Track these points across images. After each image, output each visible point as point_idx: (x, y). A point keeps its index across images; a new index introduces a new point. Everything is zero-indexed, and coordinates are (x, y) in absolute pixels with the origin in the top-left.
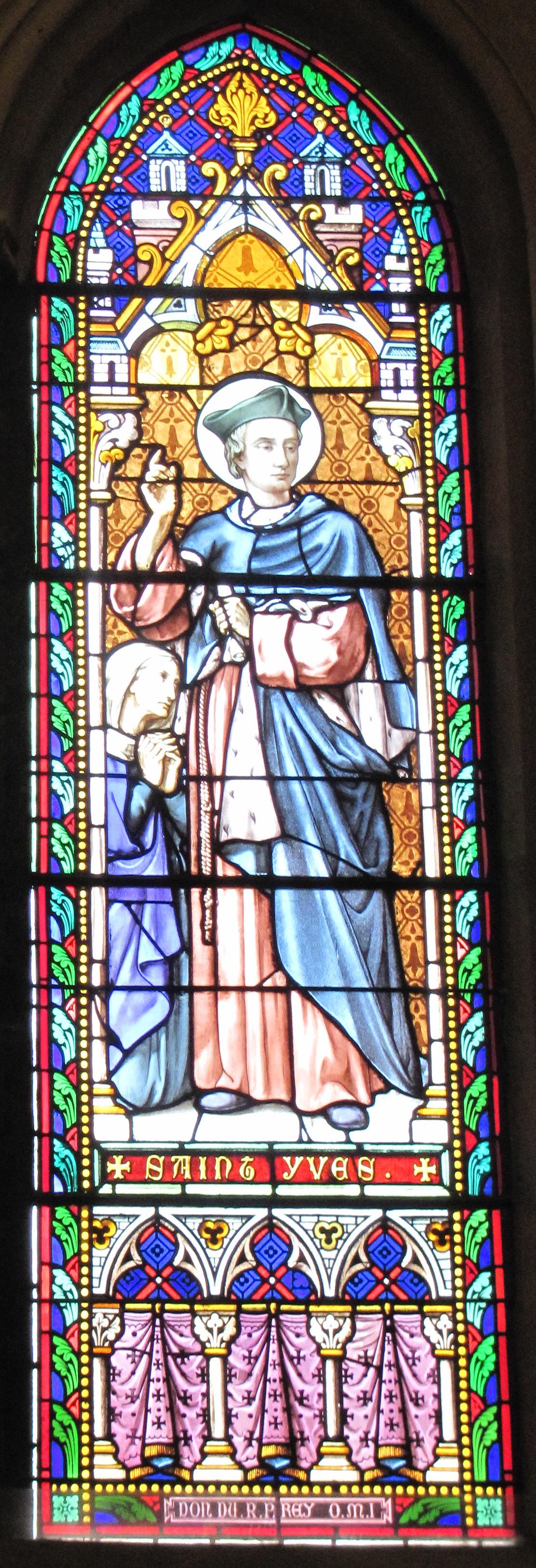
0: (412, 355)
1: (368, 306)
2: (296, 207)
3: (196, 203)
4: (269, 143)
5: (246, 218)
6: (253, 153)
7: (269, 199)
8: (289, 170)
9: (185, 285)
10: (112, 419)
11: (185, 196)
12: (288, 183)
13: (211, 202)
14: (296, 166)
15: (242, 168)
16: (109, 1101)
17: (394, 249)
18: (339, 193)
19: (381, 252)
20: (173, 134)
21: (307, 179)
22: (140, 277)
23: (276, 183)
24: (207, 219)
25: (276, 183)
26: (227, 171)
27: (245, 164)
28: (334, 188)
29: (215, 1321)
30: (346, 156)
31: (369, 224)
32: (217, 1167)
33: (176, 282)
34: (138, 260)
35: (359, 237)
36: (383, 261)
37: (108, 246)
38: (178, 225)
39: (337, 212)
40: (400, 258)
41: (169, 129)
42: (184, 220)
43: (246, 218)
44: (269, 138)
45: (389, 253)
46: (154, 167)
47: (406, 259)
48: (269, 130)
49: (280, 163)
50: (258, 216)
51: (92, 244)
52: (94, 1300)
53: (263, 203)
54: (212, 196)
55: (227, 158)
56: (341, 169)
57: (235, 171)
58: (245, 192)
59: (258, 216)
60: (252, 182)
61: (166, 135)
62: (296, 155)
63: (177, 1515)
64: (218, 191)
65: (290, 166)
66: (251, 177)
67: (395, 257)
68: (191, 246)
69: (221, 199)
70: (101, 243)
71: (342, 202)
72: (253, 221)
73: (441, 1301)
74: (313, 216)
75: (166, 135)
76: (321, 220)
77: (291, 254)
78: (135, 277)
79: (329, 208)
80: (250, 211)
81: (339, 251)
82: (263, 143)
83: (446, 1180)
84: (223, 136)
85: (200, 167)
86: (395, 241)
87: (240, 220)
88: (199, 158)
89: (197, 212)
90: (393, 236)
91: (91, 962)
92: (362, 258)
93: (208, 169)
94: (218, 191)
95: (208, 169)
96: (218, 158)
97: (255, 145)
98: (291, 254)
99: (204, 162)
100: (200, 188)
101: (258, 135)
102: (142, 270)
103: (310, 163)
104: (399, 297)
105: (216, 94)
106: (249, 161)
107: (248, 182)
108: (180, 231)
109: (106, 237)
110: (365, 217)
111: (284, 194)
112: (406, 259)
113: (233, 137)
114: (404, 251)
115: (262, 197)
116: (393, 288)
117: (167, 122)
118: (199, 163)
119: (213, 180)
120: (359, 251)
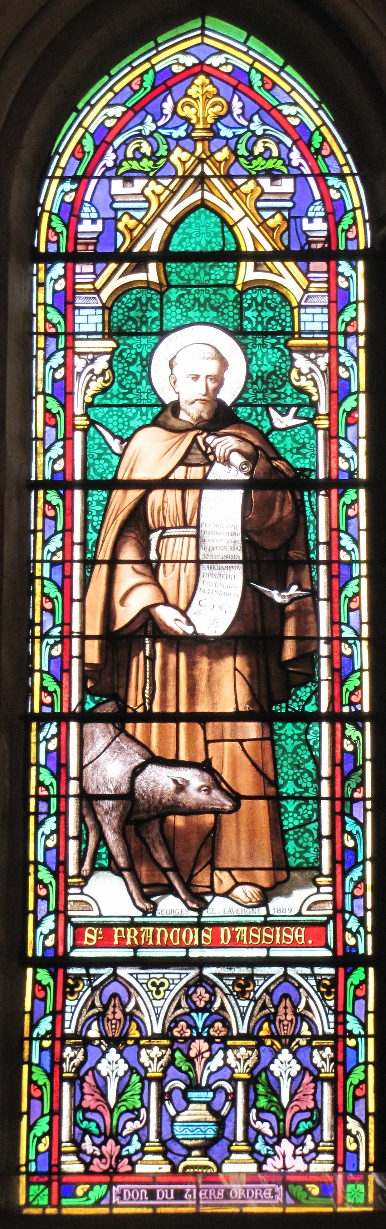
5: (203, 195)
7: (219, 177)
9: (151, 251)
22: (118, 246)
29: (156, 1052)
32: (158, 937)
33: (145, 249)
43: (203, 195)
52: (65, 1037)
53: (215, 181)
58: (202, 173)
63: (122, 1199)
72: (208, 196)
73: (326, 1037)
77: (236, 224)
80: (206, 187)
83: (331, 943)
87: (196, 197)
98: (236, 224)
115: (215, 176)
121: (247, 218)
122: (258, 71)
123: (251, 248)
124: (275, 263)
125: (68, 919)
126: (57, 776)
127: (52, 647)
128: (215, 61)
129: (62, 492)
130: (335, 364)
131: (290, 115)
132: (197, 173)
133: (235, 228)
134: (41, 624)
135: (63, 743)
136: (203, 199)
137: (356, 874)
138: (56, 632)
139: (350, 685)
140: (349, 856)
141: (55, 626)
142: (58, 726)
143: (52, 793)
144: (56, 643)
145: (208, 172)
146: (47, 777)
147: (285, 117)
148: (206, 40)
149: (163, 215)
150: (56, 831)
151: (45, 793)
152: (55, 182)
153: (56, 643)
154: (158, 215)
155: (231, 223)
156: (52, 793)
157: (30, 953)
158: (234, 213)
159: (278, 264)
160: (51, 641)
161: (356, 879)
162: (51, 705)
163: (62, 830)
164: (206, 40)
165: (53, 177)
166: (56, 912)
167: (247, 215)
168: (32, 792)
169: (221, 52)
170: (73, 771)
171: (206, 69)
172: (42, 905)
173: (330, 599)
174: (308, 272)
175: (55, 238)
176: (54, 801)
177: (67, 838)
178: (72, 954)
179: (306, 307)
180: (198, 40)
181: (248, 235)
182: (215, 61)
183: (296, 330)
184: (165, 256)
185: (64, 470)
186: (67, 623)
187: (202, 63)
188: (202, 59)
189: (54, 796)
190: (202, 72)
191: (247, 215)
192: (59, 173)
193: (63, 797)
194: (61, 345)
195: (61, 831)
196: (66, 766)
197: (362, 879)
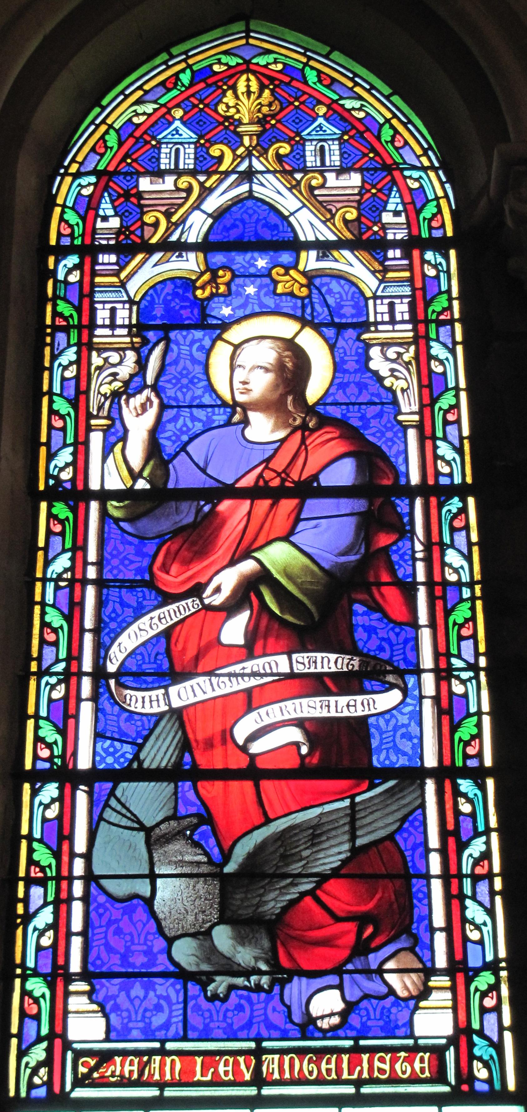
0: (407, 291)
1: (366, 255)
2: (298, 176)
3: (202, 178)
4: (273, 126)
5: (251, 187)
6: (259, 136)
8: (292, 146)
9: (189, 241)
10: (114, 357)
11: (193, 173)
12: (291, 157)
13: (215, 177)
14: (297, 142)
15: (247, 149)
16: (85, 999)
17: (391, 207)
18: (338, 163)
19: (378, 209)
20: (184, 123)
21: (308, 153)
23: (279, 158)
24: (211, 190)
25: (279, 158)
26: (234, 151)
27: (250, 146)
28: (334, 158)
30: (344, 133)
31: (368, 187)
34: (144, 224)
35: (358, 198)
36: (380, 216)
37: (116, 215)
38: (184, 195)
39: (337, 179)
40: (396, 213)
41: (181, 119)
42: (189, 190)
43: (251, 187)
44: (273, 122)
45: (385, 210)
46: (164, 150)
47: (403, 214)
48: (273, 117)
49: (284, 141)
50: (262, 185)
51: (101, 213)
54: (216, 172)
55: (234, 139)
56: (340, 144)
57: (240, 151)
58: (250, 166)
59: (262, 185)
60: (258, 158)
61: (177, 124)
62: (298, 134)
64: (223, 168)
65: (293, 142)
66: (257, 154)
67: (391, 214)
68: (197, 213)
69: (227, 174)
70: (110, 212)
71: (341, 171)
74: (314, 183)
75: (177, 124)
76: (323, 186)
77: (292, 214)
78: (142, 237)
79: (331, 177)
80: (255, 180)
81: (337, 210)
82: (268, 126)
84: (231, 124)
85: (208, 149)
86: (391, 200)
88: (207, 141)
89: (201, 184)
90: (389, 196)
91: (73, 855)
92: (360, 215)
93: (215, 151)
94: (223, 168)
95: (215, 151)
96: (226, 141)
97: (260, 129)
98: (292, 214)
99: (212, 145)
100: (206, 165)
101: (263, 121)
102: (148, 231)
103: (311, 140)
104: (395, 244)
105: (224, 92)
106: (255, 142)
107: (253, 158)
108: (187, 199)
109: (114, 208)
110: (363, 181)
111: (287, 168)
112: (403, 214)
113: (240, 122)
114: (400, 208)
116: (390, 237)
117: (178, 113)
118: (207, 145)
119: (220, 159)
120: (358, 209)
121: (305, 209)
122: (312, 68)
123: (311, 238)
124: (342, 251)
125: (67, 1045)
126: (57, 855)
127: (53, 687)
128: (262, 60)
129: (71, 503)
130: (423, 358)
131: (353, 109)
132: (243, 167)
133: (292, 219)
134: (39, 659)
135: (67, 810)
136: (251, 191)
137: (477, 847)
138: (60, 667)
139: (466, 732)
140: (466, 825)
141: (58, 661)
142: (61, 789)
143: (49, 874)
144: (59, 682)
145: (257, 165)
146: (43, 855)
147: (349, 111)
148: (251, 41)
149: (203, 207)
150: (54, 926)
151: (40, 875)
152: (68, 179)
153: (59, 682)
154: (197, 207)
155: (287, 213)
156: (49, 874)
157: (12, 1093)
158: (288, 202)
159: (347, 253)
160: (53, 680)
161: (476, 855)
162: (50, 759)
163: (62, 922)
164: (251, 41)
165: (66, 174)
166: (51, 1037)
167: (304, 206)
168: (22, 873)
169: (268, 52)
170: (80, 845)
171: (252, 67)
172: (31, 1026)
173: (432, 625)
174: (386, 259)
175: (68, 231)
176: (51, 886)
177: (69, 934)
178: (73, 1095)
179: (382, 298)
180: (243, 42)
181: (307, 225)
182: (262, 60)
183: (372, 319)
184: (206, 247)
185: (73, 480)
186: (74, 656)
187: (247, 62)
188: (247, 58)
189: (52, 878)
190: (248, 71)
191: (304, 206)
192: (74, 168)
193: (64, 878)
194: (74, 340)
195: (59, 925)
196: (71, 838)
197: (486, 855)
